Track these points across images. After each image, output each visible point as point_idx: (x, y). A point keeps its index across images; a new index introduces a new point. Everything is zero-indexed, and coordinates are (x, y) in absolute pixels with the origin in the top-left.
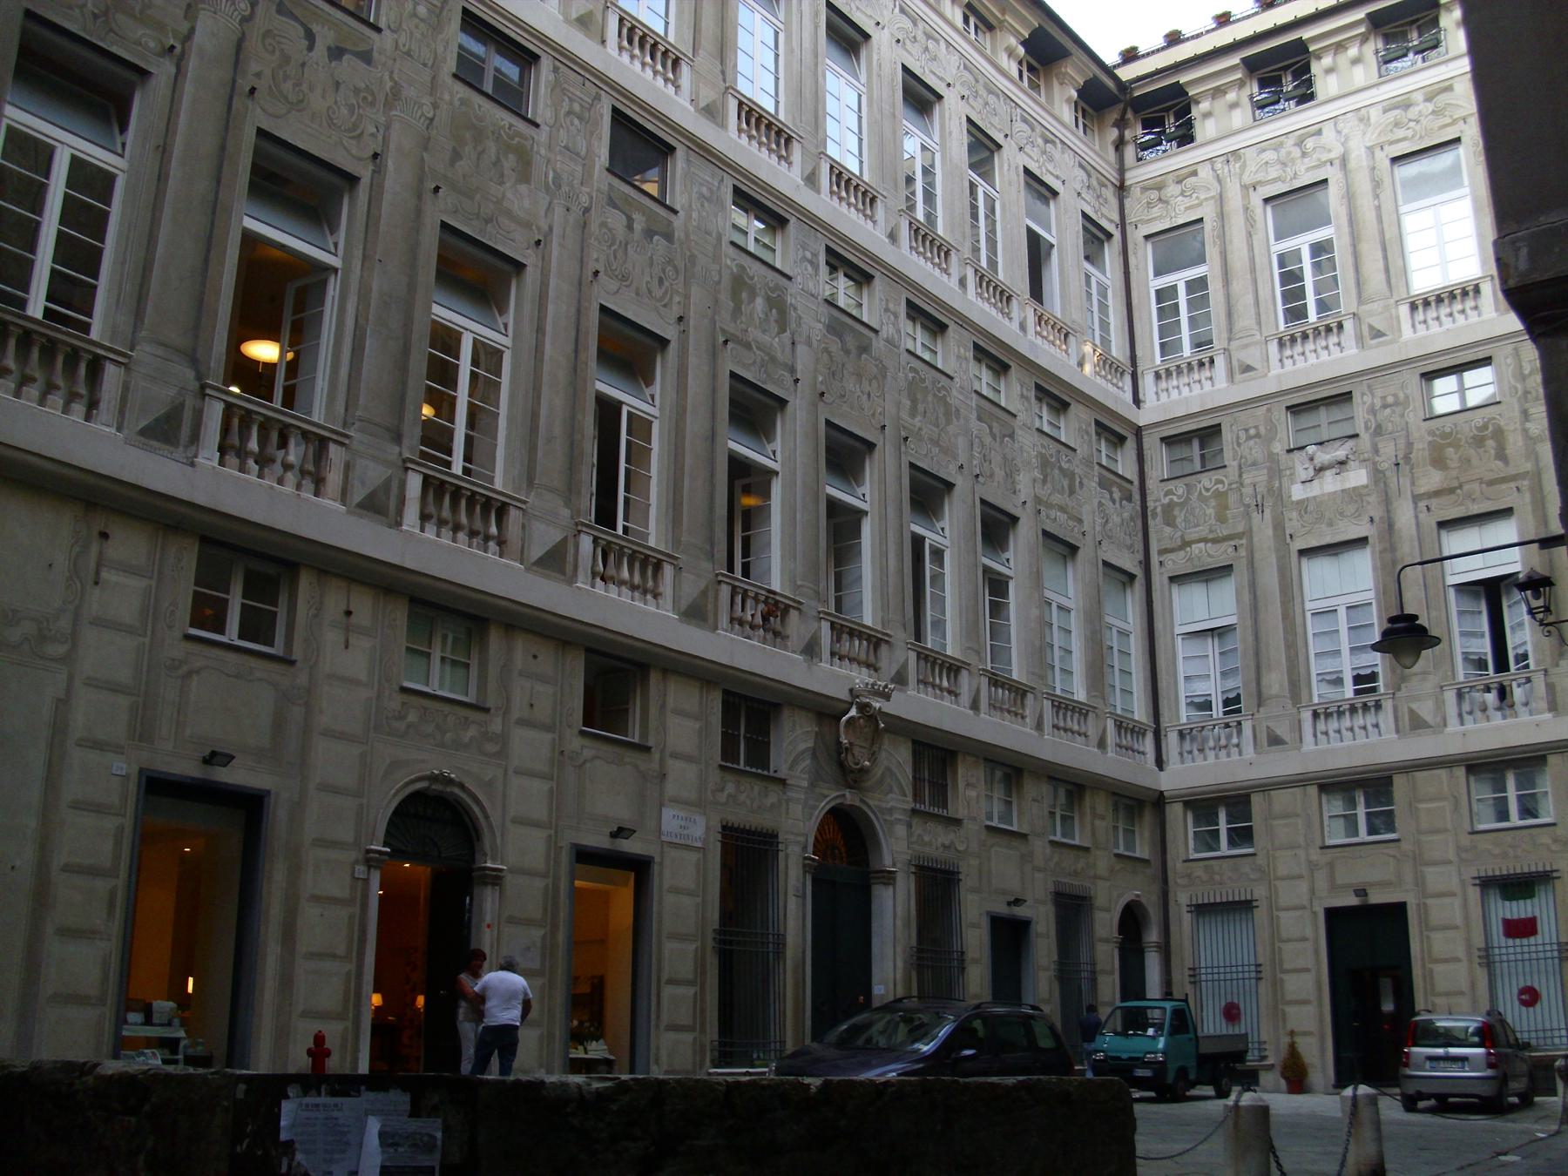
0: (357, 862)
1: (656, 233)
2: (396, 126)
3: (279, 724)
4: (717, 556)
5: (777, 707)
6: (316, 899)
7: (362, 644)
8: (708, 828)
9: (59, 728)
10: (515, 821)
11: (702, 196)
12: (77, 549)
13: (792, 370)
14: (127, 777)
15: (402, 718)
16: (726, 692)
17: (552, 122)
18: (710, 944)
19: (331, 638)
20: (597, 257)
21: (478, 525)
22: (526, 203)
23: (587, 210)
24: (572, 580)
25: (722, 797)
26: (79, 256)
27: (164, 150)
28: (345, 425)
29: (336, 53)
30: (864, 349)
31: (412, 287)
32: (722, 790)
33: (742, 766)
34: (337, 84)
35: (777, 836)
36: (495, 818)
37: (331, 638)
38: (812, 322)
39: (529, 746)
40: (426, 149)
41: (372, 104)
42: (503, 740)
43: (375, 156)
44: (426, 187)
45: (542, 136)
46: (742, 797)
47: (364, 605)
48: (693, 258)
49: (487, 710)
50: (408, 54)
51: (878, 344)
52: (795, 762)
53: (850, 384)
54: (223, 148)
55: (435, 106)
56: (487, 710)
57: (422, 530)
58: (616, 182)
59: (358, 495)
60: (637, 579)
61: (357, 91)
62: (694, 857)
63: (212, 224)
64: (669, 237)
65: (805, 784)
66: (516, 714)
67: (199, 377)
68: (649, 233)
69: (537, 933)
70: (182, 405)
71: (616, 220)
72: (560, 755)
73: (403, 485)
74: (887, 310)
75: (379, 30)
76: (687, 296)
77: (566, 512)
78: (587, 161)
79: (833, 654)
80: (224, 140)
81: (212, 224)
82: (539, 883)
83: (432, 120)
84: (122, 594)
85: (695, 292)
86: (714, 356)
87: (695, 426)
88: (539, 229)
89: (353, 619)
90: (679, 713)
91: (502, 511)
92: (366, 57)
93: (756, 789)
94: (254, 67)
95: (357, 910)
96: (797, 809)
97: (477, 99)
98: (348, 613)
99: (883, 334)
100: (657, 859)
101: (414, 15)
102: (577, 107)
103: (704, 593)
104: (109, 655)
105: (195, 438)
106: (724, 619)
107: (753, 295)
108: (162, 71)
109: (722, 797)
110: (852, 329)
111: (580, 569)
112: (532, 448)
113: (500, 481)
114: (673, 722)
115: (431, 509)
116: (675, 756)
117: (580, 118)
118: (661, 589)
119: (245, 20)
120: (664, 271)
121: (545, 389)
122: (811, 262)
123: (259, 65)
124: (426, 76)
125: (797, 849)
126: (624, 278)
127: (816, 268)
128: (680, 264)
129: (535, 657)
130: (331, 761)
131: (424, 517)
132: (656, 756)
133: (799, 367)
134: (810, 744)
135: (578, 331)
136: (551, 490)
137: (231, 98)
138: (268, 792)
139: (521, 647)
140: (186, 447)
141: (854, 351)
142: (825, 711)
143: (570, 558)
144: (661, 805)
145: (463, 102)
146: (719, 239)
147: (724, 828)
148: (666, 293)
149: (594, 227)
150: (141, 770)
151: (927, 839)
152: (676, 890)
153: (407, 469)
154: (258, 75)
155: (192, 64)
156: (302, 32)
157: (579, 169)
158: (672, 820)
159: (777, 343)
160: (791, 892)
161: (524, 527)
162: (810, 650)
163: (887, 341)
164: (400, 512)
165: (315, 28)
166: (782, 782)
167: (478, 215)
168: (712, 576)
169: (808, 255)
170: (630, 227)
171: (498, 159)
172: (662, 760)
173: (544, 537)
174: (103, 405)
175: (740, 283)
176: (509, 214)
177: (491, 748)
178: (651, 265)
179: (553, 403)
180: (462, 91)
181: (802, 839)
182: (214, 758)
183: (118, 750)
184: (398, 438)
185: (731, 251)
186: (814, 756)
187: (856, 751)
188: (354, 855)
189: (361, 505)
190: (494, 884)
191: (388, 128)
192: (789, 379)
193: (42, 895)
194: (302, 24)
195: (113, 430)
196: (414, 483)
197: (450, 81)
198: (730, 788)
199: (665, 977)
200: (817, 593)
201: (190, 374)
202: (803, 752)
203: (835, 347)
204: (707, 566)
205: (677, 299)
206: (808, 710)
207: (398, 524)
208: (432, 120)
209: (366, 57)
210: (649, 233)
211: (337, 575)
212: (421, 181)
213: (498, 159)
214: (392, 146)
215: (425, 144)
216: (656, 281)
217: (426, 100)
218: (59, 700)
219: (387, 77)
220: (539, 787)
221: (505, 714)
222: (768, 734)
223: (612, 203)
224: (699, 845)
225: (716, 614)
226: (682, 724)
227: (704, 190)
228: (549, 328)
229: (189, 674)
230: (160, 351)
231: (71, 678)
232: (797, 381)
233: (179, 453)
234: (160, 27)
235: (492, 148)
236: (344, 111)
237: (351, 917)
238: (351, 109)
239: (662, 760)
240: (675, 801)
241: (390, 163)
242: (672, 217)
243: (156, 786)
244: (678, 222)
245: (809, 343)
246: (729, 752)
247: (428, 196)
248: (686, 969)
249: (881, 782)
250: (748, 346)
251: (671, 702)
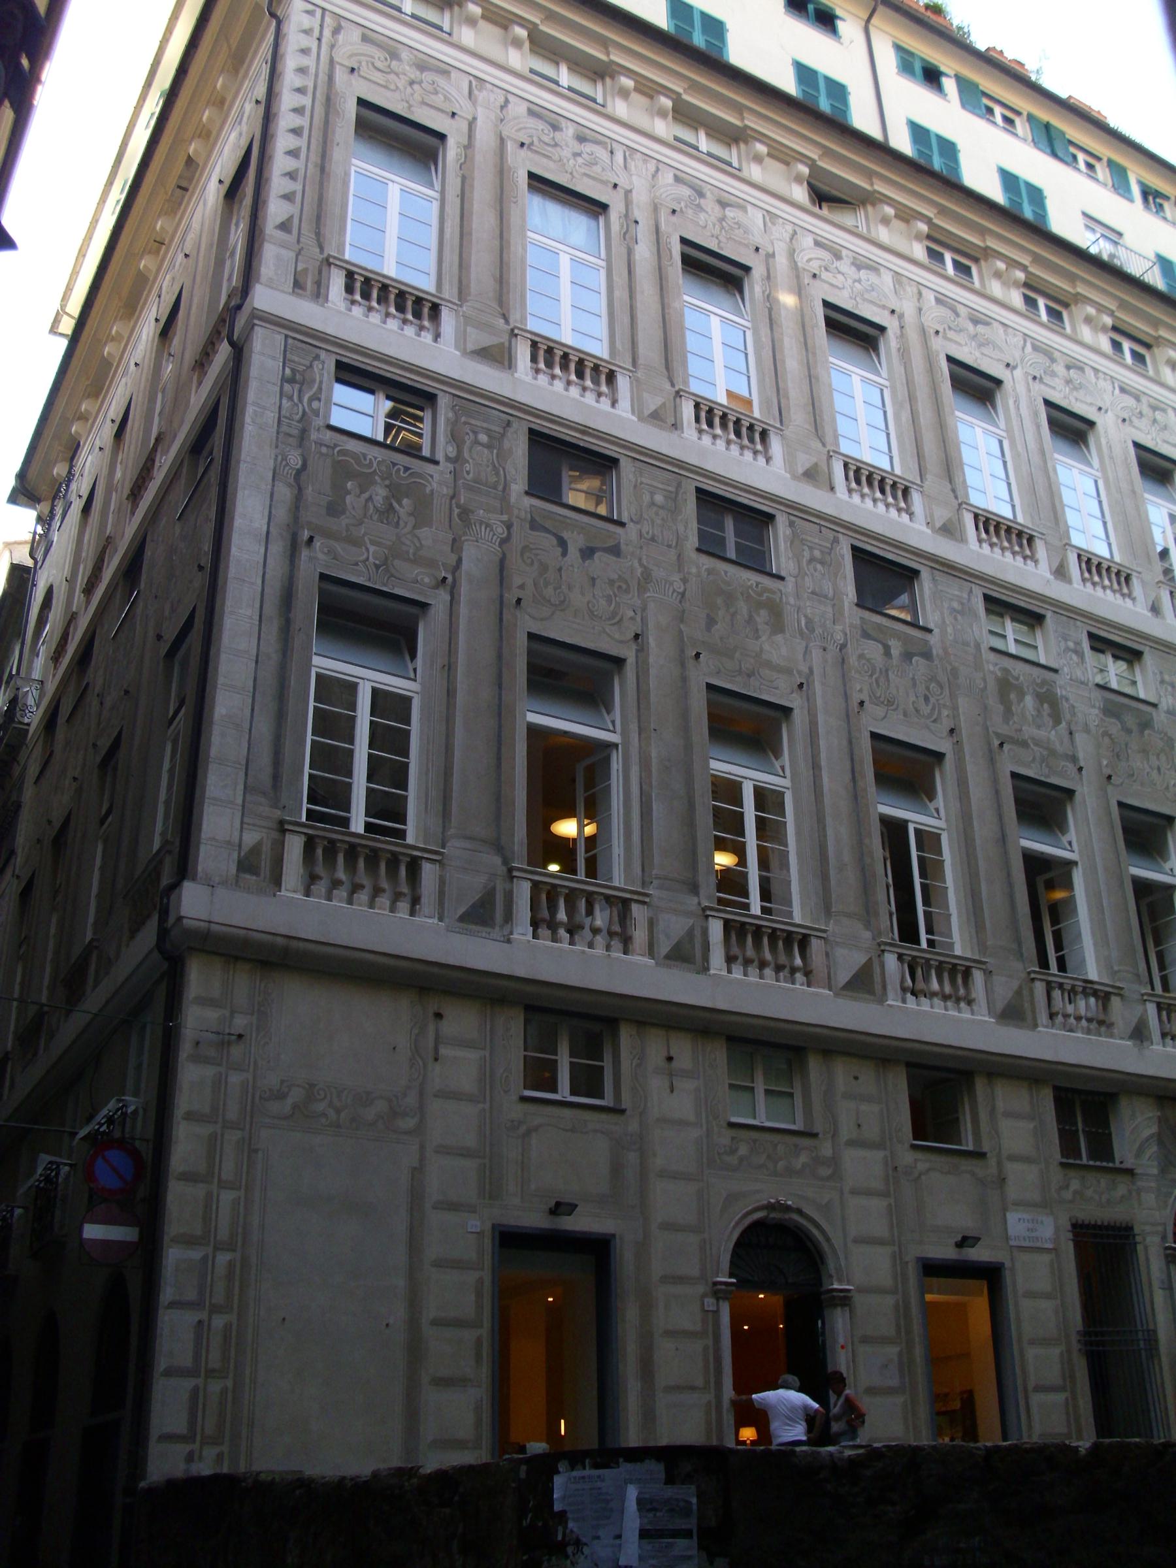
0: (704, 1296)
1: (914, 655)
2: (651, 606)
3: (617, 1169)
4: (1025, 955)
6: (671, 1334)
7: (686, 1086)
8: (1057, 1229)
9: (416, 1197)
10: (858, 1241)
11: (953, 610)
12: (416, 1031)
13: (1074, 759)
14: (480, 1234)
15: (733, 1151)
16: (1056, 1089)
17: (796, 572)
18: (1076, 1346)
19: (656, 1084)
20: (860, 688)
21: (782, 959)
22: (784, 651)
23: (843, 647)
24: (882, 1000)
25: (1068, 1195)
26: (389, 772)
27: (449, 668)
28: (644, 884)
29: (588, 553)
30: (1146, 724)
31: (688, 747)
32: (1067, 1187)
33: (1085, 1161)
34: (593, 579)
35: (1131, 1228)
36: (837, 1242)
37: (656, 1084)
38: (1087, 710)
39: (862, 1166)
40: (682, 621)
41: (627, 591)
42: (834, 1162)
43: (637, 636)
44: (687, 656)
45: (789, 586)
46: (1089, 1193)
47: (683, 1049)
48: (954, 672)
49: (815, 1135)
50: (653, 539)
51: (1160, 718)
52: (1139, 1153)
53: (1137, 762)
54: (500, 657)
55: (685, 581)
56: (814, 1135)
57: (729, 971)
58: (867, 615)
59: (664, 948)
60: (948, 989)
61: (611, 582)
62: (1046, 1258)
63: (500, 727)
64: (927, 655)
65: (1155, 1171)
66: (845, 1134)
67: (505, 862)
68: (908, 656)
69: (893, 1351)
70: (494, 888)
71: (873, 650)
72: (893, 1170)
73: (705, 932)
74: (1162, 682)
75: (622, 524)
76: (955, 708)
77: (867, 935)
78: (836, 600)
79: (1164, 1035)
80: (500, 648)
81: (500, 727)
82: (890, 1300)
83: (683, 594)
84: (461, 1066)
85: (963, 703)
86: (992, 761)
87: (984, 831)
88: (799, 672)
89: (675, 1064)
90: (1008, 1114)
91: (804, 942)
92: (615, 551)
93: (1103, 1182)
94: (517, 581)
95: (710, 1342)
96: (1150, 1199)
97: (722, 566)
98: (670, 1059)
99: (1163, 706)
100: (1008, 1264)
101: (653, 504)
102: (817, 553)
103: (1019, 993)
104: (453, 1123)
105: (508, 918)
106: (1043, 1017)
107: (1021, 695)
108: (439, 601)
109: (1068, 1195)
110: (1129, 708)
111: (889, 987)
112: (825, 877)
113: (799, 915)
114: (1005, 1125)
115: (735, 950)
116: (1012, 1158)
117: (822, 563)
118: (973, 995)
119: (504, 542)
120: (928, 688)
121: (829, 820)
122: (1076, 652)
123: (522, 576)
124: (672, 555)
125: (1157, 1239)
126: (890, 703)
127: (1081, 655)
128: (943, 678)
129: (856, 1078)
130: (670, 1200)
131: (730, 960)
132: (992, 1161)
133: (1081, 755)
134: (1154, 1129)
135: (852, 760)
136: (849, 915)
137: (501, 614)
138: (614, 1236)
139: (842, 1072)
140: (502, 927)
141: (1135, 728)
143: (877, 978)
144: (1005, 1210)
145: (710, 572)
146: (978, 646)
147: (1075, 1226)
148: (933, 709)
149: (853, 660)
150: (494, 1226)
152: (1031, 1295)
153: (707, 917)
154: (522, 587)
155: (464, 589)
156: (555, 542)
157: (830, 609)
158: (1017, 1224)
159: (1055, 736)
160: (1156, 1284)
161: (827, 954)
162: (1139, 1034)
163: (1168, 712)
164: (706, 958)
165: (566, 535)
166: (1130, 1172)
167: (740, 672)
168: (1023, 975)
169: (1071, 644)
170: (887, 652)
171: (751, 617)
172: (999, 1164)
173: (849, 962)
174: (424, 900)
175: (1006, 687)
176: (768, 664)
177: (824, 1172)
178: (914, 685)
179: (839, 832)
180: (706, 562)
181: (1160, 1228)
182: (559, 1208)
183: (472, 1209)
184: (694, 889)
185: (992, 656)
186: (1161, 1143)
188: (701, 1289)
189: (668, 957)
190: (843, 1305)
191: (644, 609)
192: (1071, 769)
193: (415, 1350)
194: (555, 535)
195: (436, 921)
196: (716, 929)
197: (694, 555)
198: (1075, 1185)
199: (1031, 1385)
200: (1138, 975)
201: (498, 860)
203: (1114, 728)
204: (1019, 966)
205: (945, 713)
206: (1147, 1095)
207: (706, 969)
208: (683, 594)
209: (615, 551)
210: (908, 656)
211: (653, 1025)
212: (682, 651)
213: (751, 617)
214: (651, 625)
215: (681, 617)
216: (922, 700)
217: (676, 578)
218: (415, 1169)
219: (636, 564)
220: (877, 1205)
221: (833, 1136)
222: (1107, 1125)
223: (866, 635)
224: (1051, 1246)
225: (1034, 1011)
226: (1015, 1127)
227: (955, 605)
228: (823, 763)
229: (528, 1133)
230: (467, 844)
231: (422, 1147)
232: (1080, 769)
233: (496, 933)
234: (431, 564)
235: (743, 607)
236: (603, 602)
237: (706, 1348)
238: (609, 600)
239: (999, 1164)
240: (1017, 1204)
241: (651, 640)
242: (927, 636)
243: (510, 1240)
244: (934, 640)
245: (1087, 730)
246: (1069, 1146)
247: (691, 663)
248: (1053, 1374)
250: (1024, 744)
251: (1000, 1105)
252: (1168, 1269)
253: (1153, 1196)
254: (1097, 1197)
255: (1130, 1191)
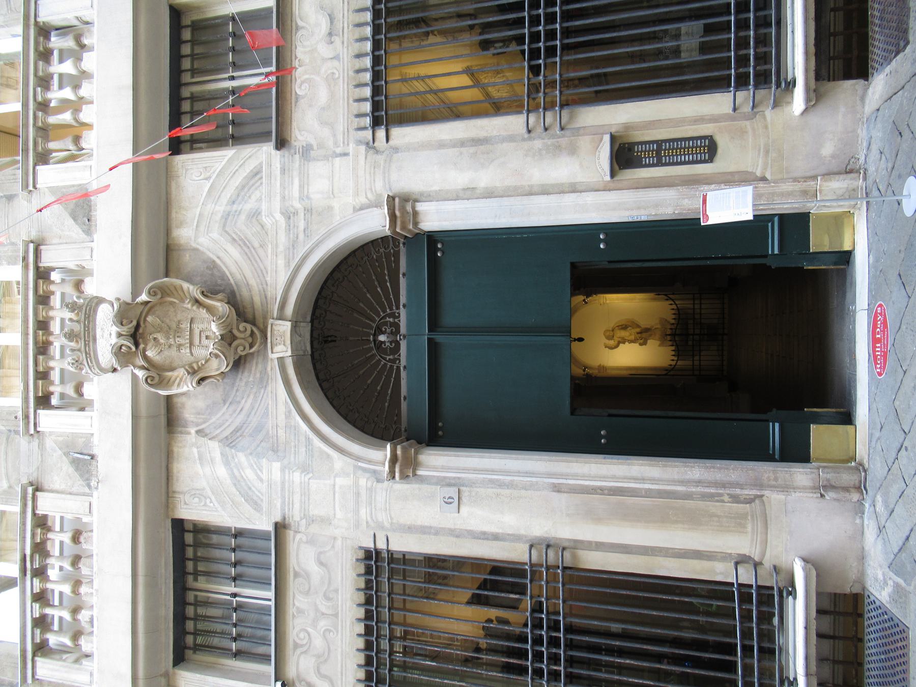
5: (179, 526)
65: (276, 466)
134: (214, 448)
142: (159, 428)
151: (323, 95)
166: (280, 528)
181: (363, 482)
186: (230, 441)
187: (201, 353)
202: (227, 463)
206: (169, 456)
249: (242, 243)
252: (423, 480)
253: (314, 484)
254: (323, 624)
255: (311, 542)
